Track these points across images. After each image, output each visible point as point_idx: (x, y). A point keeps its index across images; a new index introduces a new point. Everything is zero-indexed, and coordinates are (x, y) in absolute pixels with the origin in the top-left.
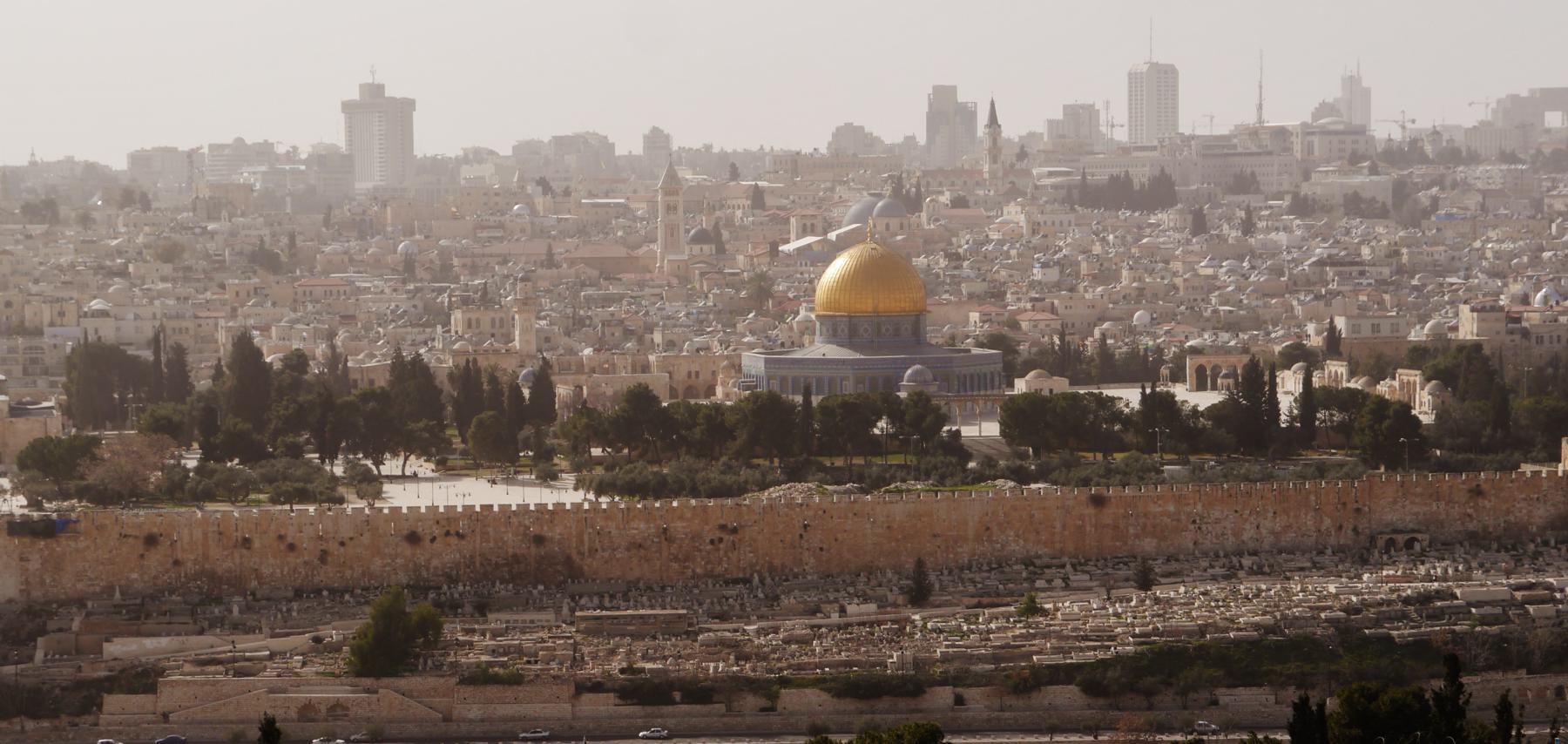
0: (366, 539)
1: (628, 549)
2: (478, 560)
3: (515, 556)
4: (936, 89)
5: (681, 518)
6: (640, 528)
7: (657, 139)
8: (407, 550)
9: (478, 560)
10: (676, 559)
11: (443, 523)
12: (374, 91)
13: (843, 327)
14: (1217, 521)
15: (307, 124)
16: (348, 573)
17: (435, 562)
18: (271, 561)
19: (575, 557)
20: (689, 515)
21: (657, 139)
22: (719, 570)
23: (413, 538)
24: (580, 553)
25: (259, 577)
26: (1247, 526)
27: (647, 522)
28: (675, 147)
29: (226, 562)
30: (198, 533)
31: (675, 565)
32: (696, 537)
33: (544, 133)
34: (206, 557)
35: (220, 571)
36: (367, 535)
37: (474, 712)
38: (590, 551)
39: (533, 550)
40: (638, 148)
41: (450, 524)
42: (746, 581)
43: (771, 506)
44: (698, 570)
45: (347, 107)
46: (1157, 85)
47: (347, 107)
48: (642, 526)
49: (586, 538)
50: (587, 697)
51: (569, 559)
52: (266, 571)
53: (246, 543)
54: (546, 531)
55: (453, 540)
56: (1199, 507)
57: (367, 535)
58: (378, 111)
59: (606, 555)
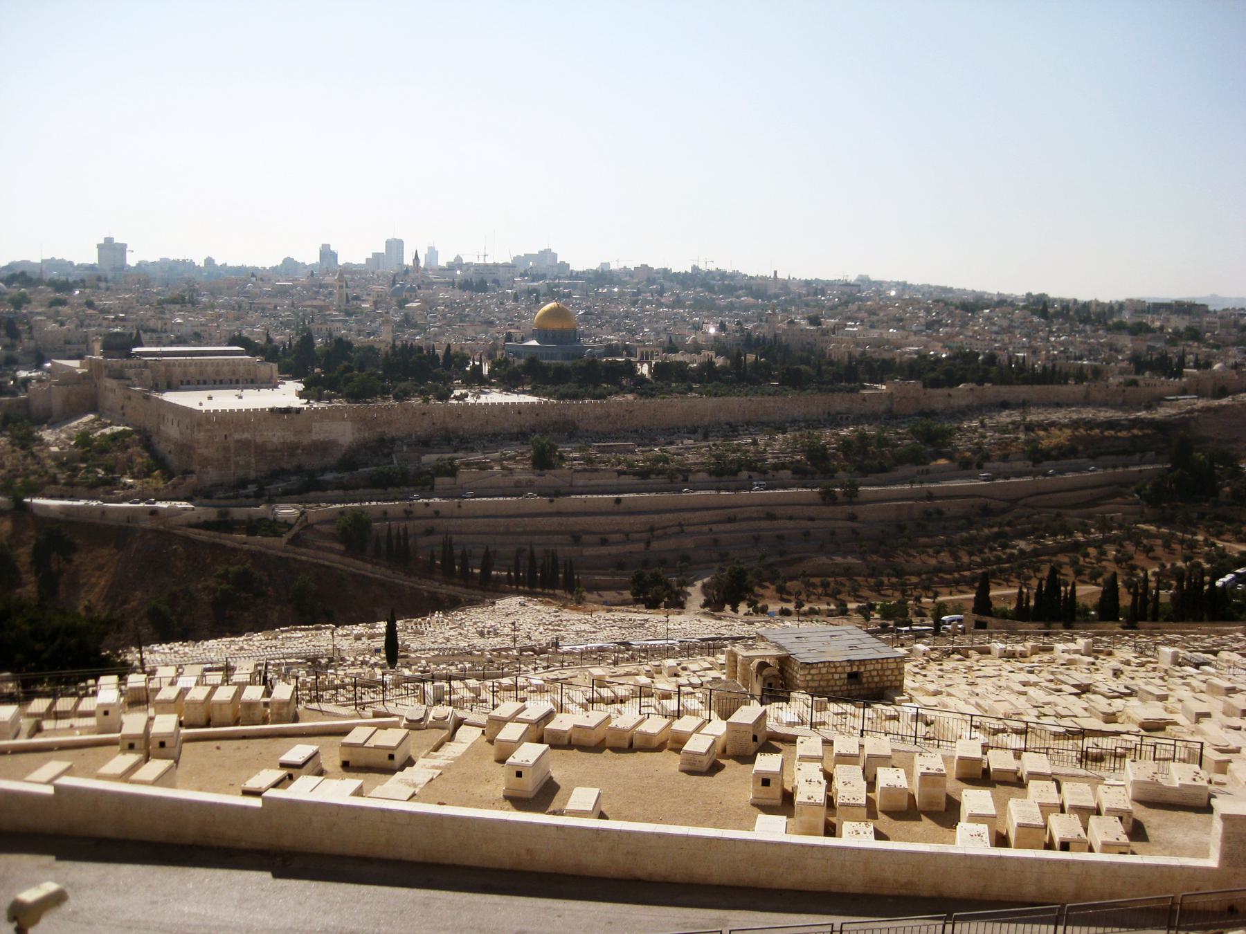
6: (599, 411)
7: (209, 261)
12: (109, 241)
13: (540, 334)
15: (84, 254)
21: (209, 261)
28: (340, 262)
29: (451, 424)
33: (174, 256)
37: (581, 483)
40: (202, 265)
41: (504, 407)
42: (636, 431)
43: (620, 403)
45: (99, 246)
46: (395, 246)
47: (99, 246)
53: (460, 416)
58: (111, 249)
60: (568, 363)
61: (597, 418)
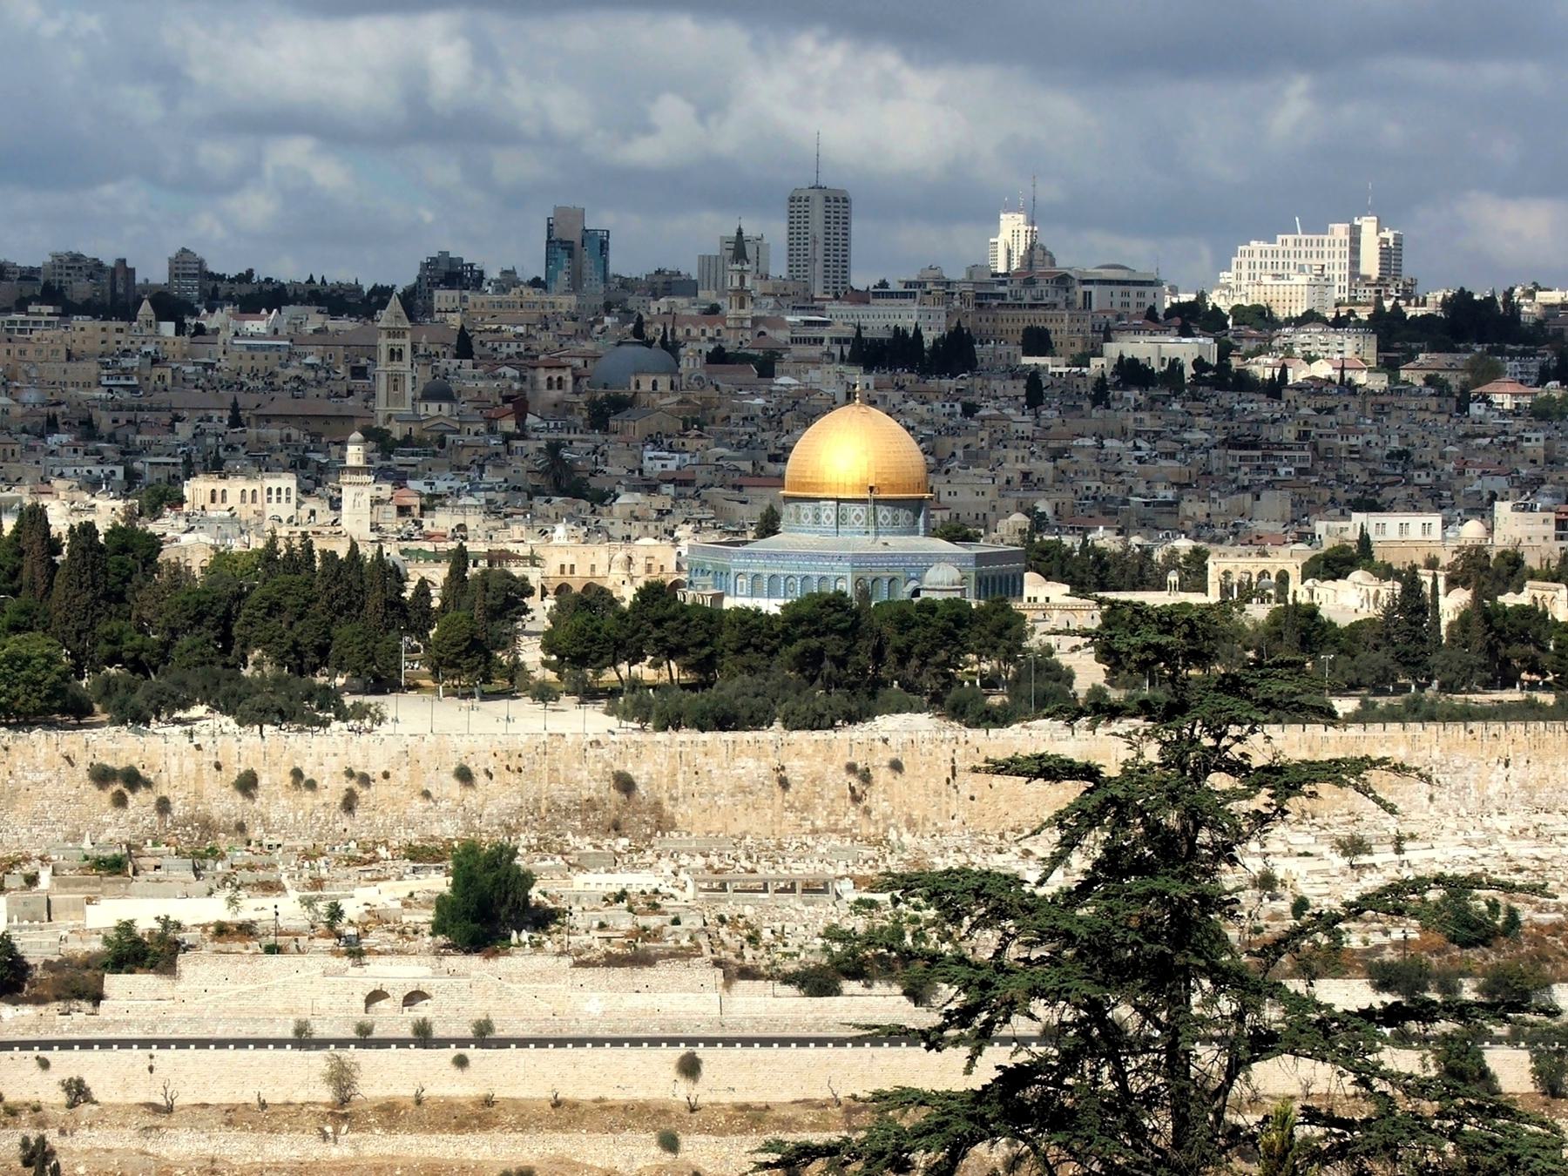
2: (544, 804)
4: (561, 212)
8: (454, 787)
9: (544, 804)
10: (791, 806)
14: (1458, 770)
16: (379, 820)
17: (491, 809)
18: (283, 802)
19: (667, 807)
20: (810, 751)
22: (845, 823)
23: (464, 776)
24: (671, 798)
25: (265, 822)
26: (1494, 777)
29: (223, 803)
30: (190, 765)
31: (791, 816)
34: (198, 794)
35: (216, 814)
44: (820, 824)
48: (751, 764)
49: (680, 777)
50: (743, 985)
51: (658, 804)
52: (274, 816)
54: (630, 768)
56: (1436, 754)
60: (771, 606)
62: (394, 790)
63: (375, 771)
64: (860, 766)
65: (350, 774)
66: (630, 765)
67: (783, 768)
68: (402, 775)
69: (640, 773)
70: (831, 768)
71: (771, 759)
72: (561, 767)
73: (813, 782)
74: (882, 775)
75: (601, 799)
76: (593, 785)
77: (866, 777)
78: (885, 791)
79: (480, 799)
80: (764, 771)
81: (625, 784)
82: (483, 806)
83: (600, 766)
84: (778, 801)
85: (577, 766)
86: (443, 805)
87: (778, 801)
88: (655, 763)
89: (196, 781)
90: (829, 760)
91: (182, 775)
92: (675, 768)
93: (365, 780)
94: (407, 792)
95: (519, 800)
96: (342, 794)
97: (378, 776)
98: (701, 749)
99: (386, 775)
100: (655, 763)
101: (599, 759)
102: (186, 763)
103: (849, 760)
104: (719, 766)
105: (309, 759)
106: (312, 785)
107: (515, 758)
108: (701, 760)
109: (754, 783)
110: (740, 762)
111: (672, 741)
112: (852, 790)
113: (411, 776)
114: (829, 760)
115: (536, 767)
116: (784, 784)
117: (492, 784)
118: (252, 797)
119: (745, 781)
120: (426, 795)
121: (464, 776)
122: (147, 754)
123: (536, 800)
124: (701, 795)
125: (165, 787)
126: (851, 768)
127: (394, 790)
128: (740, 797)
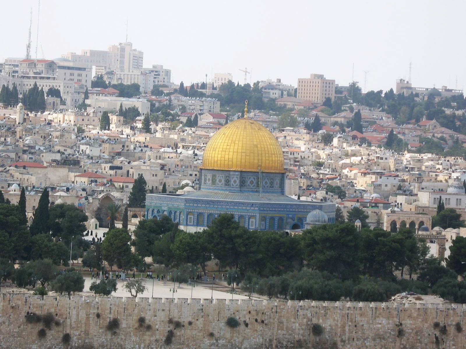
0: (200, 323)
1: (374, 340)
3: (299, 341)
5: (410, 317)
8: (227, 332)
11: (254, 313)
20: (415, 315)
23: (232, 323)
24: (343, 341)
27: (388, 318)
32: (418, 332)
36: (201, 320)
38: (349, 340)
39: (312, 337)
48: (384, 321)
49: (347, 328)
55: (259, 327)
57: (201, 320)
59: (359, 343)
61: (379, 337)
62: (194, 332)
63: (185, 319)
64: (442, 325)
65: (171, 321)
66: (321, 321)
67: (401, 324)
68: (200, 323)
69: (326, 324)
70: (426, 325)
71: (395, 319)
72: (284, 320)
73: (416, 333)
74: (452, 330)
75: (305, 341)
76: (301, 332)
77: (444, 330)
78: (453, 340)
79: (241, 339)
80: (391, 326)
81: (317, 330)
82: (242, 343)
83: (305, 320)
84: (398, 344)
85: (293, 320)
86: (221, 342)
87: (398, 344)
88: (334, 320)
89: (86, 324)
90: (425, 320)
91: (78, 322)
92: (345, 323)
93: (178, 325)
94: (201, 334)
95: (261, 340)
96: (166, 334)
97: (186, 324)
98: (358, 312)
99: (190, 323)
100: (334, 320)
101: (305, 316)
102: (80, 313)
103: (436, 321)
104: (368, 323)
105: (149, 313)
106: (149, 327)
107: (260, 315)
108: (358, 318)
109: (386, 332)
110: (378, 320)
111: (344, 306)
112: (437, 338)
113: (205, 325)
114: (425, 320)
115: (272, 320)
116: (401, 333)
117: (248, 330)
118: (114, 333)
119: (381, 332)
120: (212, 335)
121: (232, 323)
122: (59, 307)
123: (271, 341)
124: (358, 339)
125: (68, 328)
126: (436, 325)
127: (194, 332)
128: (378, 341)
